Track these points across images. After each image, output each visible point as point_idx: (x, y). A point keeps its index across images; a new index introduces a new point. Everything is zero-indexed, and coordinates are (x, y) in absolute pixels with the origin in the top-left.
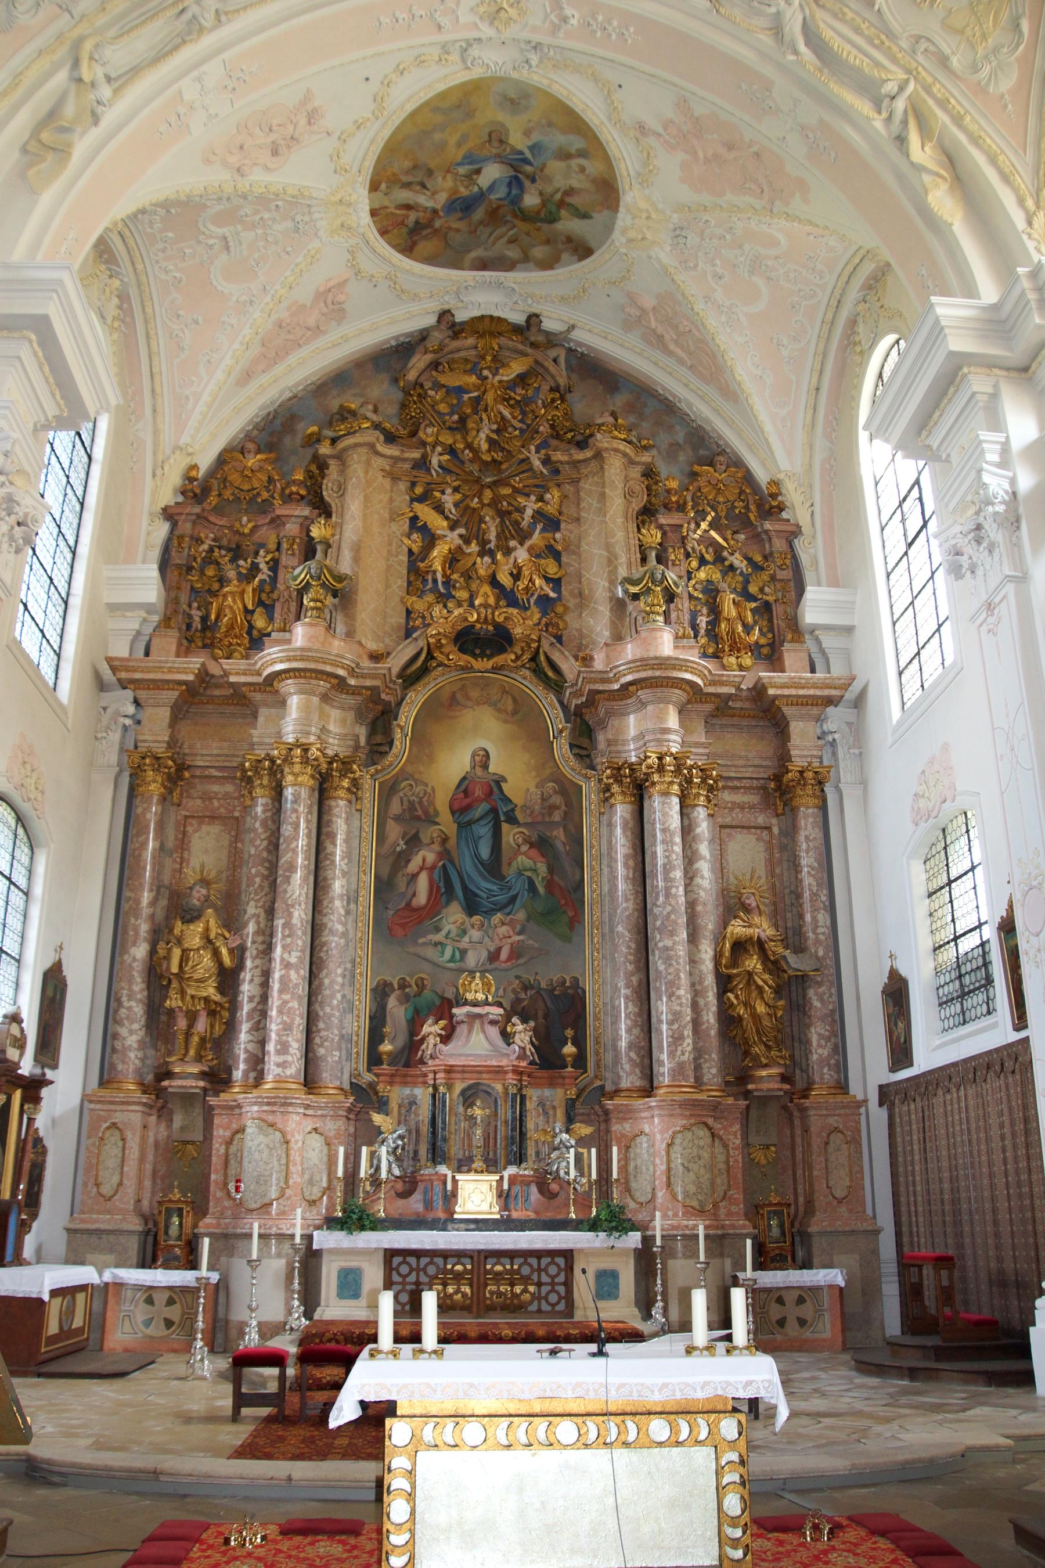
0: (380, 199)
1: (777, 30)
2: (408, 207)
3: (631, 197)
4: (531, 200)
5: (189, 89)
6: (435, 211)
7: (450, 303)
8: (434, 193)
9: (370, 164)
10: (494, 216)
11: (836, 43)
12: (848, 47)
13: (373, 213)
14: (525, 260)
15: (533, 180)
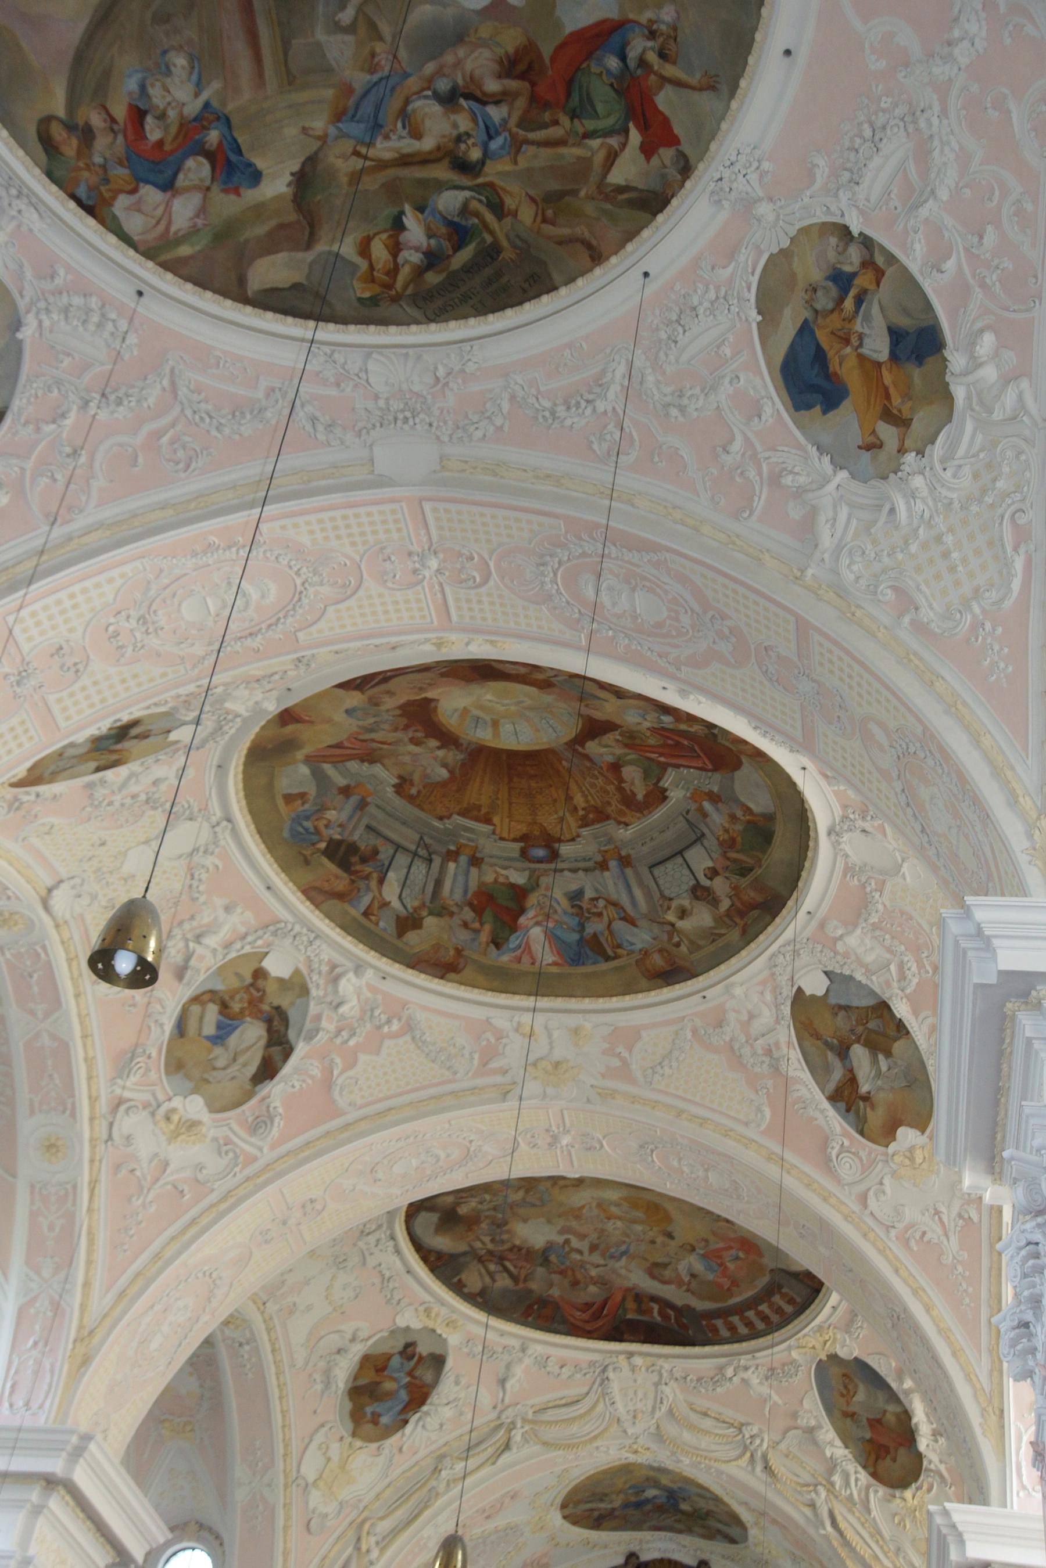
0: (567, 1512)
1: (812, 1505)
2: (592, 1510)
3: (753, 1532)
4: (684, 1506)
5: (426, 1533)
6: (614, 1510)
7: (634, 1547)
8: (611, 1502)
9: (559, 1501)
10: (661, 1509)
11: (850, 1534)
12: (857, 1538)
13: (565, 1517)
14: (689, 1531)
15: (684, 1499)
